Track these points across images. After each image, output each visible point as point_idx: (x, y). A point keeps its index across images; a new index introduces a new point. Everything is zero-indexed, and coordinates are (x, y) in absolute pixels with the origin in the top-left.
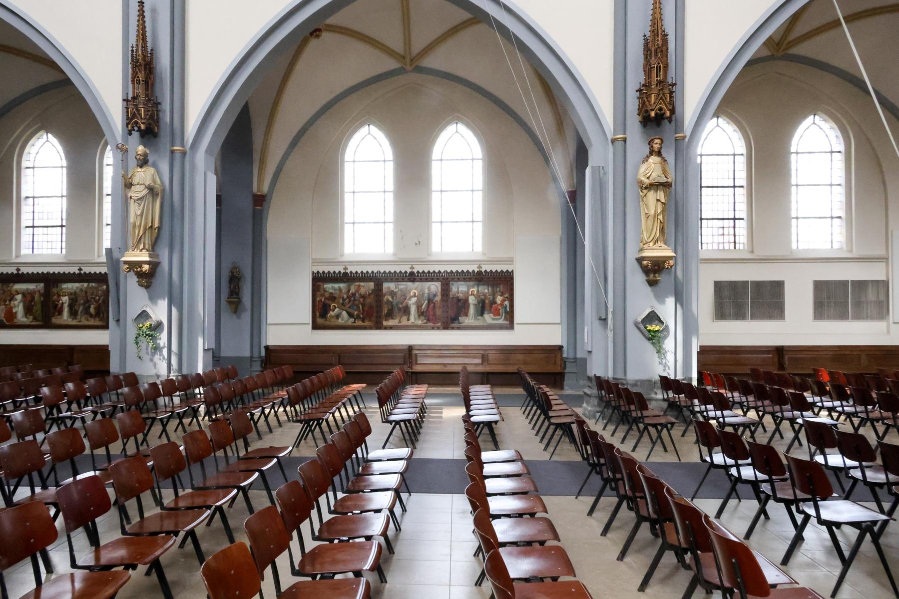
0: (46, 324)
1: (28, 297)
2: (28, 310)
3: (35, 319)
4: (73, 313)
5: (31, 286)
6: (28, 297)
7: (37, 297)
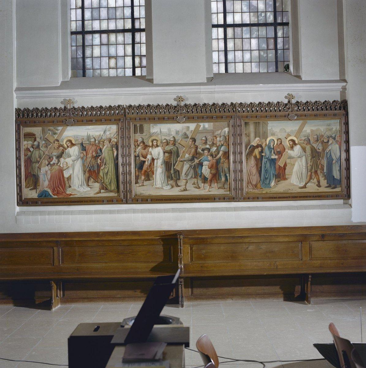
0: (124, 196)
1: (91, 152)
2: (92, 173)
3: (104, 187)
4: (172, 175)
5: (95, 131)
6: (91, 152)
7: (106, 149)
